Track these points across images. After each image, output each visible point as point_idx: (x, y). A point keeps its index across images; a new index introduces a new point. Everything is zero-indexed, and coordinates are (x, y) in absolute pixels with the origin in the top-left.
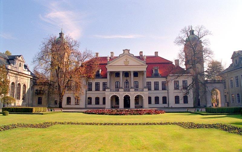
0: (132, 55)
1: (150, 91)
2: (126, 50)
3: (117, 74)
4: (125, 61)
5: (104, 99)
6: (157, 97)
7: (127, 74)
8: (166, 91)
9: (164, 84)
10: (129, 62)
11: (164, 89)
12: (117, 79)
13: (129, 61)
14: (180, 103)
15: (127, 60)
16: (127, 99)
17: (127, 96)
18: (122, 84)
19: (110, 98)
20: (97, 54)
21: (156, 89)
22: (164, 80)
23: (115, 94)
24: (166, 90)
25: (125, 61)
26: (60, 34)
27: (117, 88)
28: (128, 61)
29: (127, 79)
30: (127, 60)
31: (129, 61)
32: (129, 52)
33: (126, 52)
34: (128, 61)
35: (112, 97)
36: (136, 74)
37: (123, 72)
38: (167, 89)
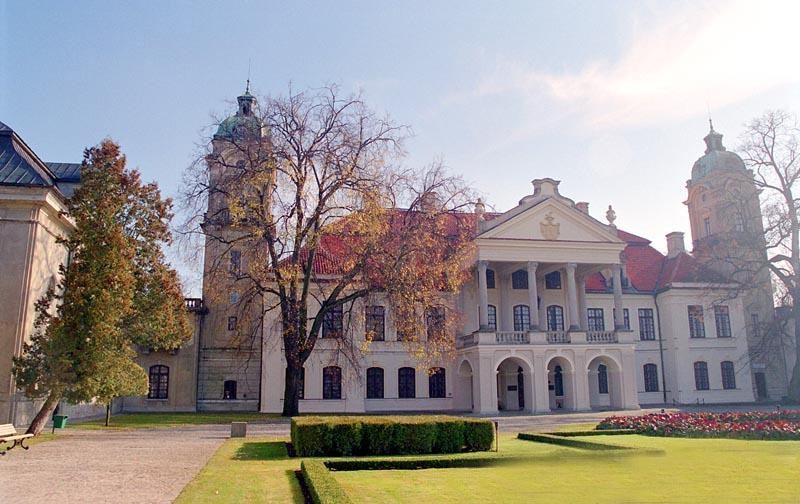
2: (548, 180)
4: (546, 222)
8: (655, 345)
9: (646, 316)
10: (561, 228)
13: (559, 225)
14: (711, 388)
22: (646, 302)
23: (514, 351)
24: (654, 339)
25: (546, 222)
26: (241, 99)
28: (554, 223)
32: (556, 190)
33: (546, 190)
34: (554, 223)
37: (541, 266)
38: (657, 338)
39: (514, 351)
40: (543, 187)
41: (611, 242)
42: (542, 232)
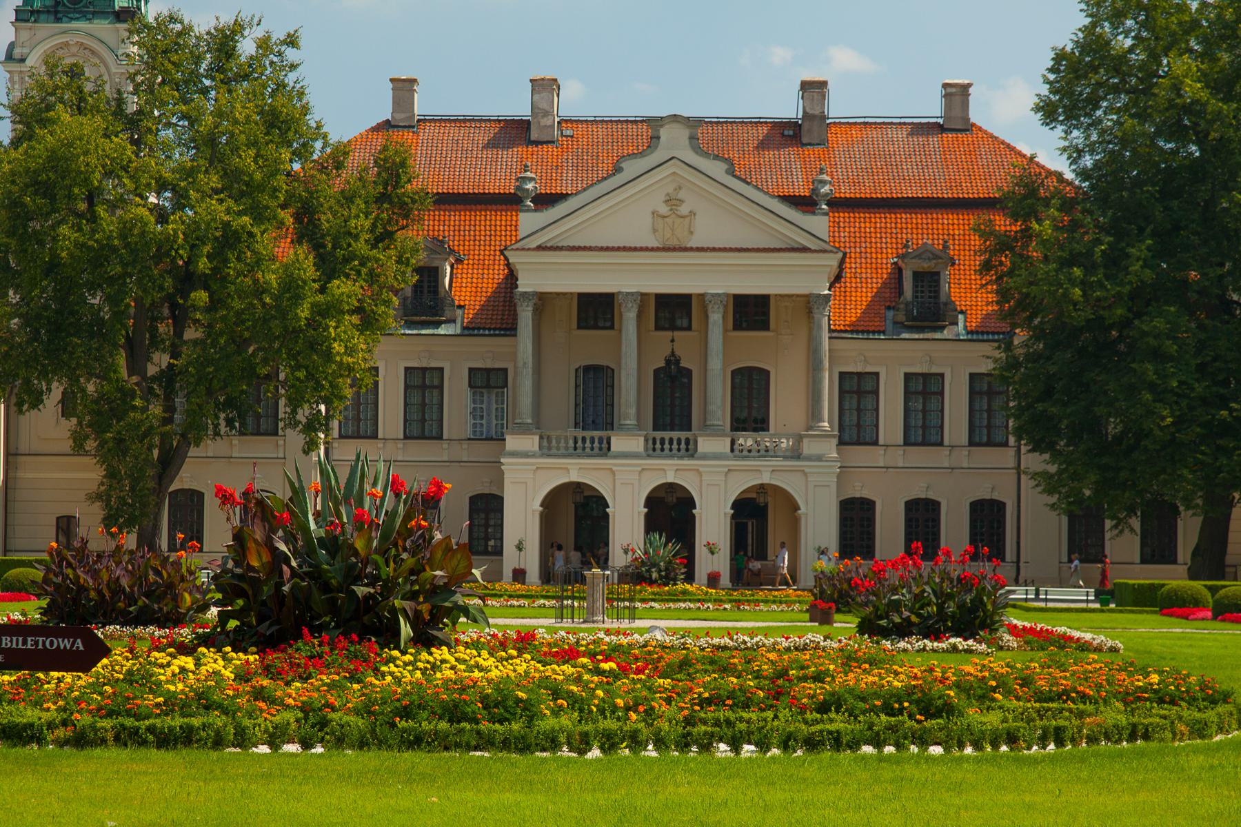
0: (725, 166)
1: (861, 455)
2: (675, 118)
3: (596, 310)
4: (664, 209)
5: (487, 509)
6: (992, 502)
7: (673, 310)
8: (1006, 457)
11: (982, 435)
12: (591, 347)
13: (692, 213)
15: (682, 201)
16: (670, 513)
17: (671, 487)
18: (632, 391)
19: (537, 506)
20: (404, 88)
21: (923, 430)
23: (577, 470)
25: (664, 209)
27: (594, 407)
28: (684, 210)
29: (677, 353)
30: (682, 201)
31: (692, 213)
35: (552, 502)
36: (751, 312)
39: (577, 470)
40: (664, 133)
41: (805, 249)
42: (655, 231)
